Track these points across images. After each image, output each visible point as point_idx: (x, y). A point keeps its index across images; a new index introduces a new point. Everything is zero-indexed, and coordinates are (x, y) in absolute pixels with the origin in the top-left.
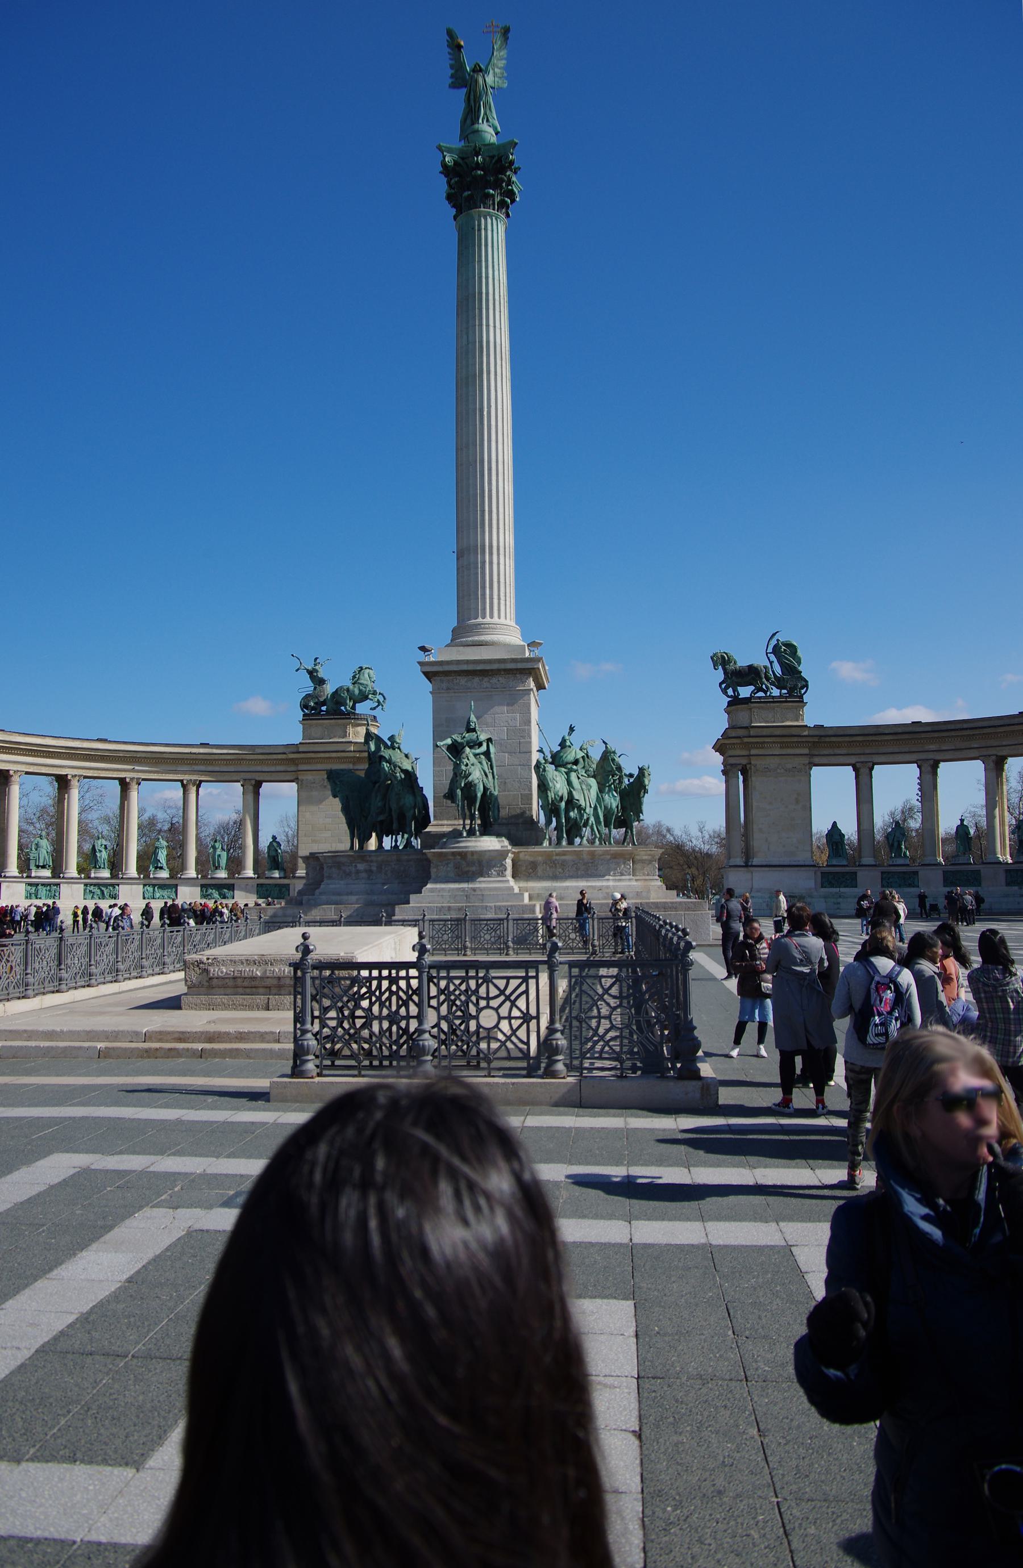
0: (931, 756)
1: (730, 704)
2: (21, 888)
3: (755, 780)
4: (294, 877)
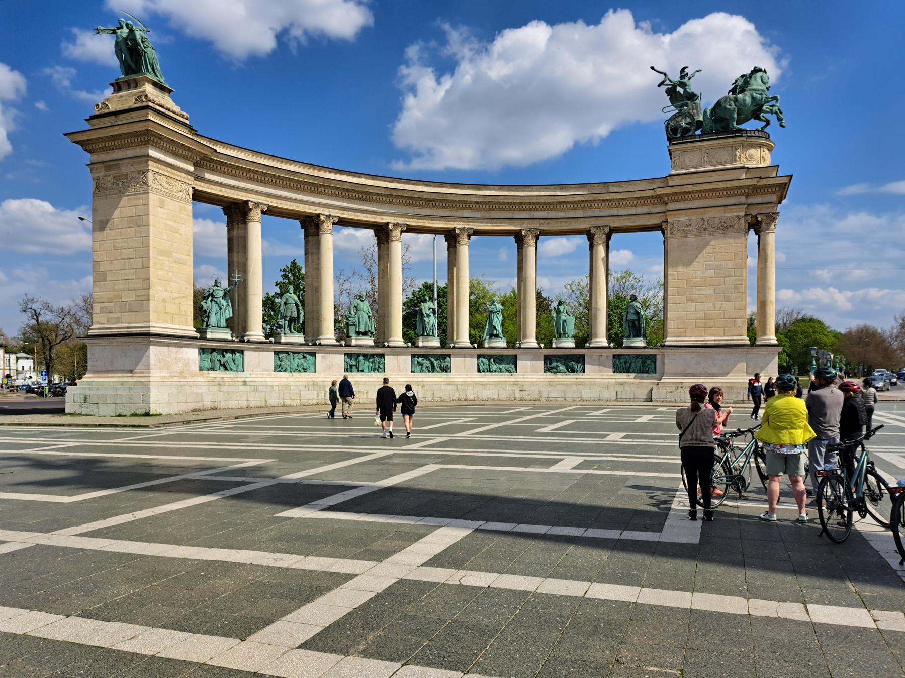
2: (339, 360)
4: (663, 346)
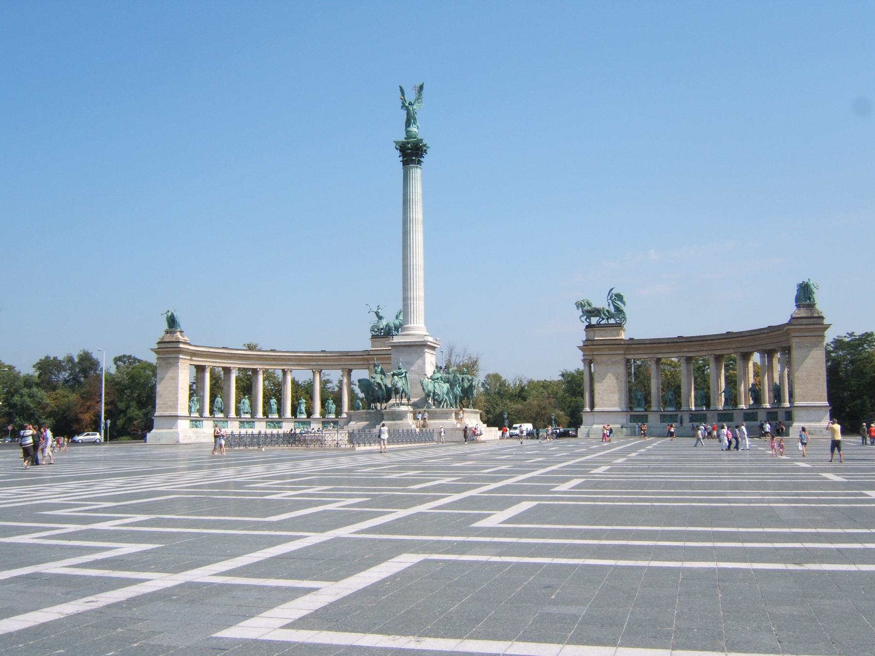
0: (684, 354)
1: (587, 327)
2: (237, 424)
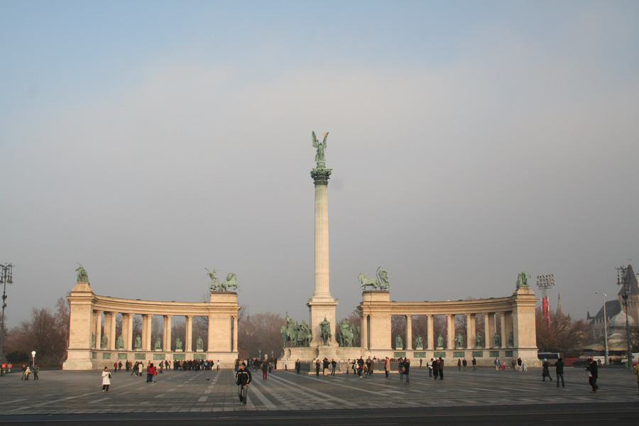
2: (116, 355)
3: (373, 321)
